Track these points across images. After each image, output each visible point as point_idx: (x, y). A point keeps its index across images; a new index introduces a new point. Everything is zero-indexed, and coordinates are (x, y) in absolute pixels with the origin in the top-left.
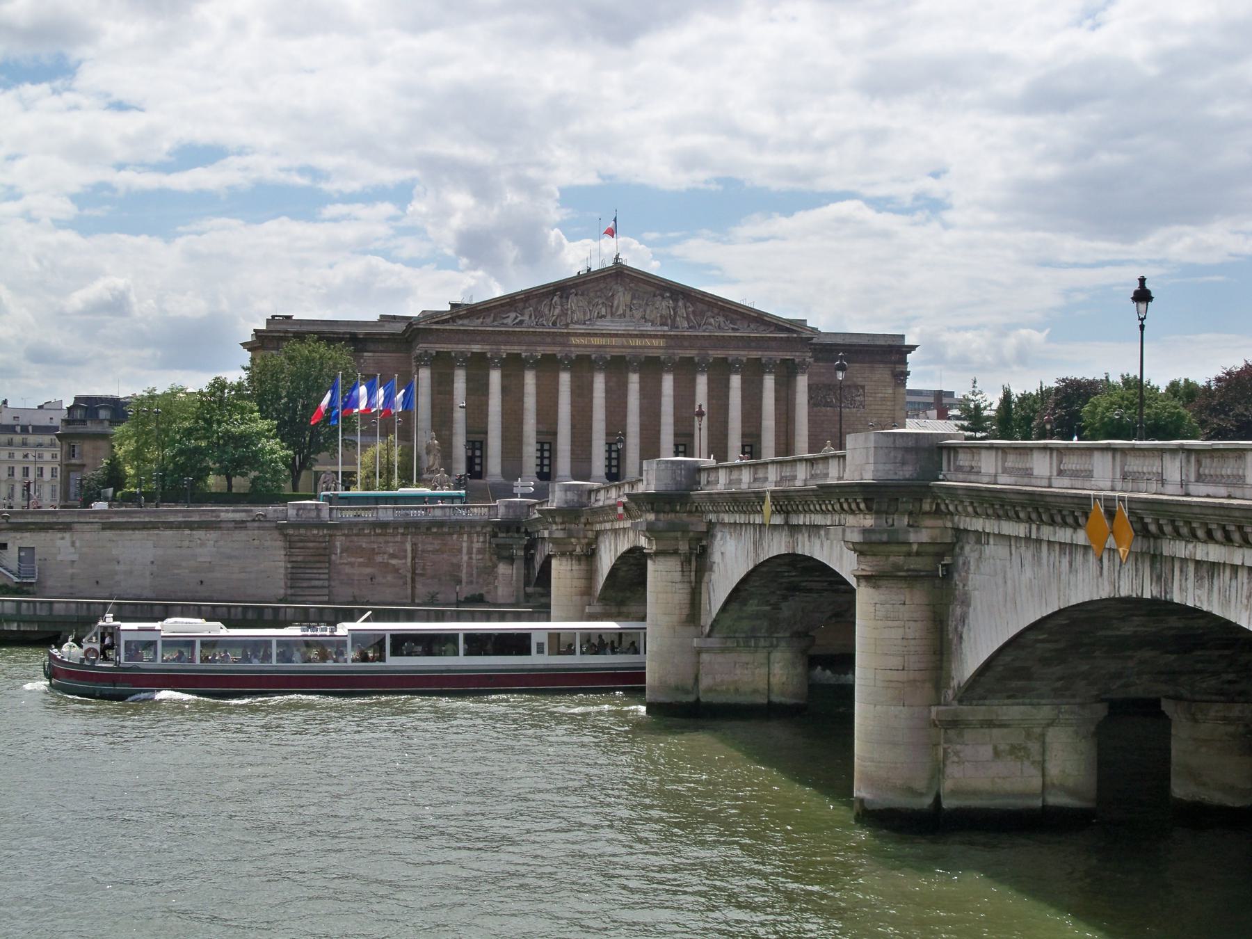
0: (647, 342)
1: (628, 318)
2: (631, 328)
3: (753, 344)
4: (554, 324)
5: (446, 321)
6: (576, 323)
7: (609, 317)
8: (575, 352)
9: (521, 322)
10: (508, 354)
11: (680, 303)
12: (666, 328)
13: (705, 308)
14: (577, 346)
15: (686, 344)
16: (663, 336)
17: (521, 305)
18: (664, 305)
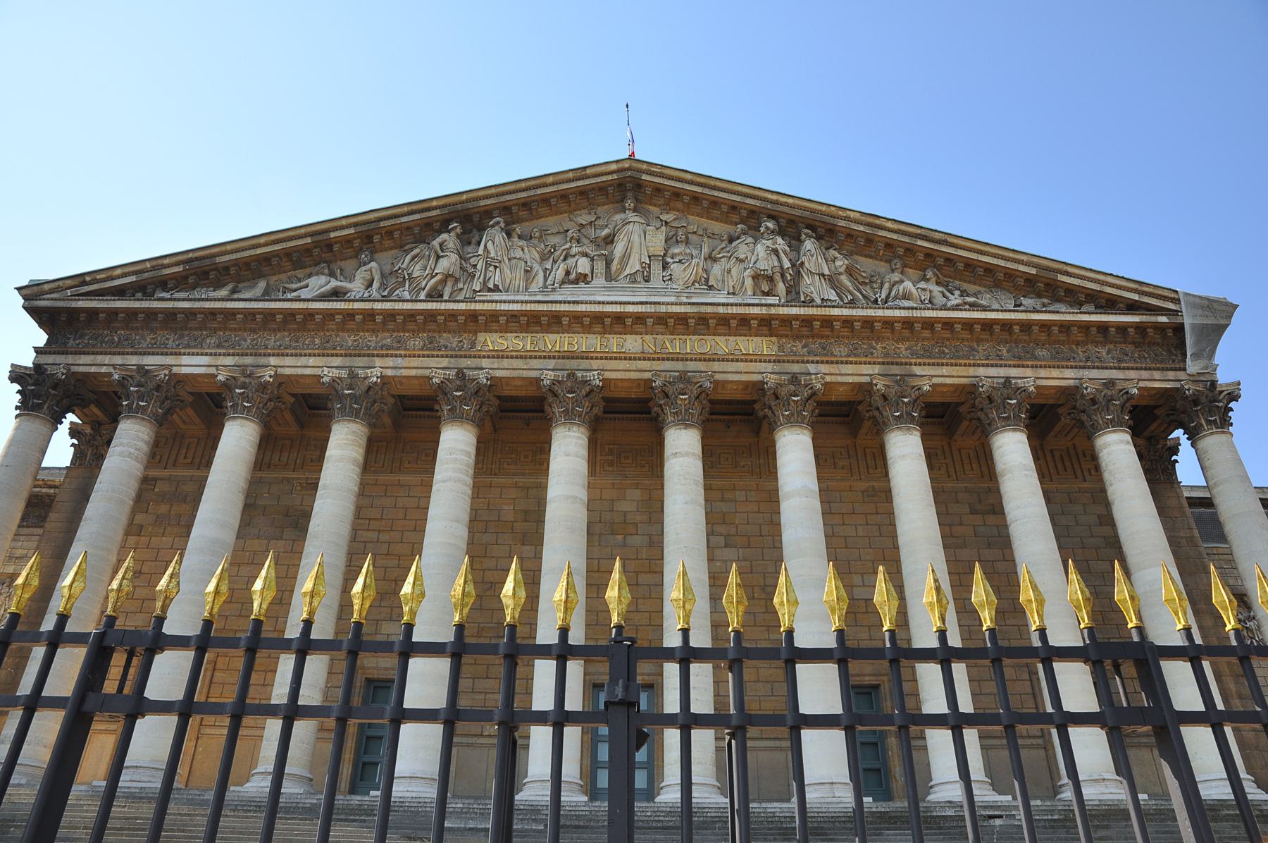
0: (722, 344)
1: (656, 281)
2: (666, 297)
3: (1041, 352)
4: (435, 295)
5: (120, 292)
6: (496, 289)
7: (600, 281)
8: (486, 370)
9: (336, 294)
10: (276, 376)
11: (809, 245)
12: (771, 300)
13: (882, 267)
14: (499, 355)
15: (840, 350)
16: (767, 325)
17: (349, 265)
18: (762, 253)
